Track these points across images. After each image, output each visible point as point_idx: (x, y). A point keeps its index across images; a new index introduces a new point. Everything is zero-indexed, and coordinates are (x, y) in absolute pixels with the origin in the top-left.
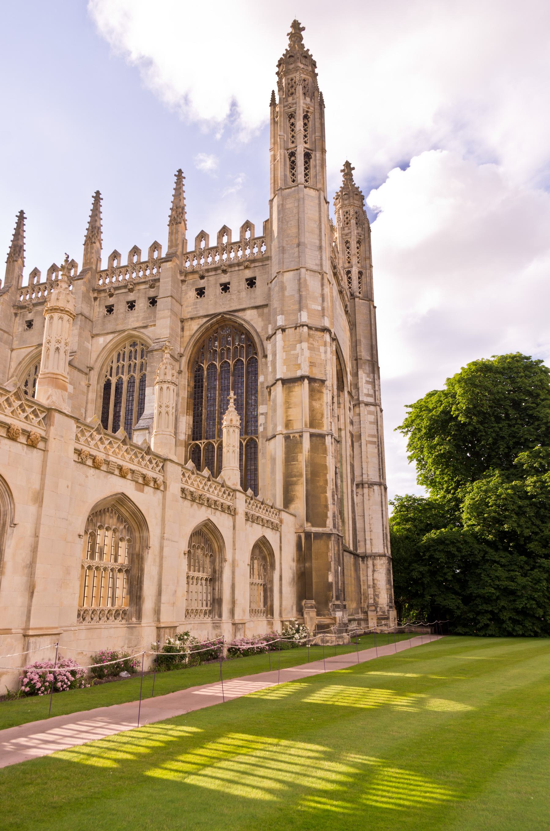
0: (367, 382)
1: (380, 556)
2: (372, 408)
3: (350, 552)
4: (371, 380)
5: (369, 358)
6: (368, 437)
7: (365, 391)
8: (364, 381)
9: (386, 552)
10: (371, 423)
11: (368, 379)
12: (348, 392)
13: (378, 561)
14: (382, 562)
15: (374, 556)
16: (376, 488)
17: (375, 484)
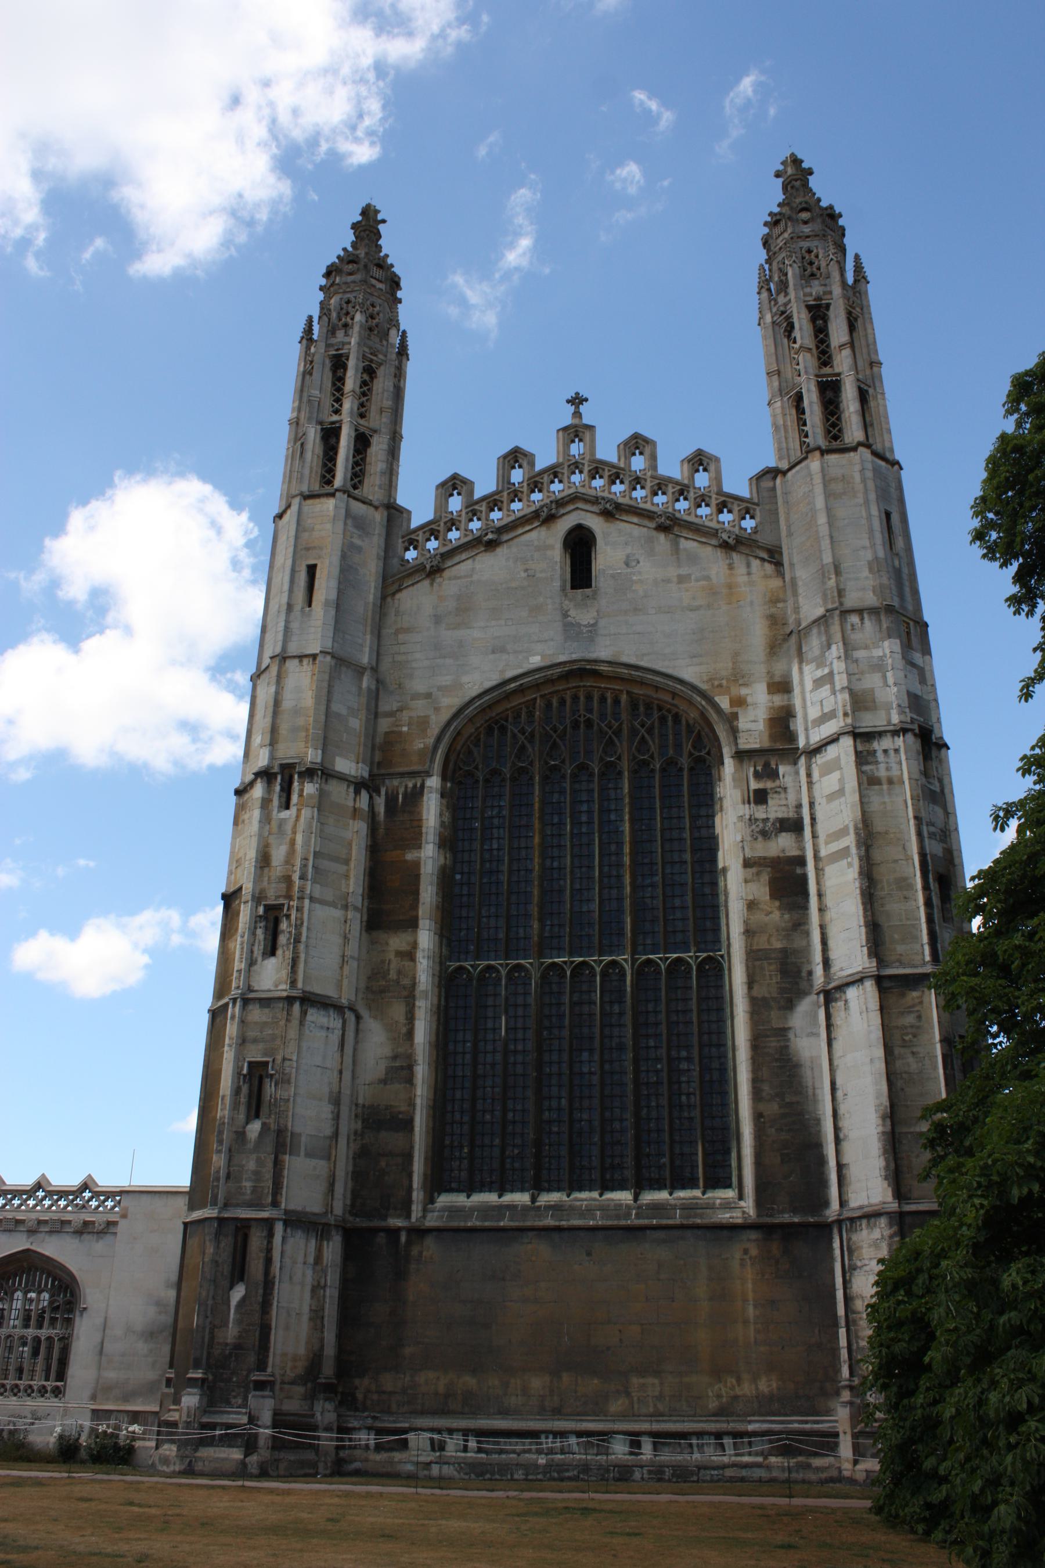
0: (818, 683)
1: (871, 1216)
2: (832, 751)
3: (733, 1228)
4: (826, 671)
5: (820, 611)
6: (827, 843)
7: (814, 713)
8: (809, 685)
9: (889, 1197)
10: (831, 797)
11: (819, 673)
12: (741, 756)
13: (865, 1232)
14: (876, 1234)
15: (851, 1222)
16: (852, 993)
17: (848, 984)
